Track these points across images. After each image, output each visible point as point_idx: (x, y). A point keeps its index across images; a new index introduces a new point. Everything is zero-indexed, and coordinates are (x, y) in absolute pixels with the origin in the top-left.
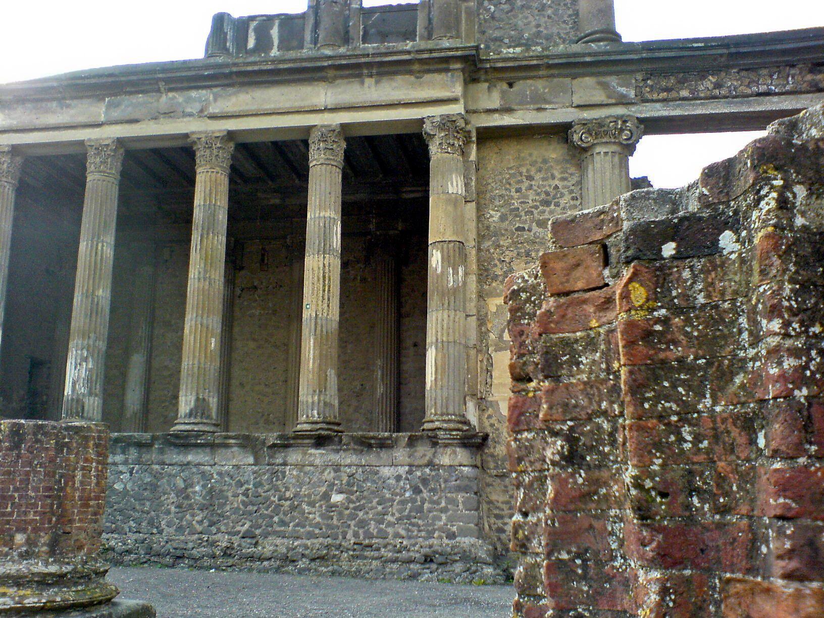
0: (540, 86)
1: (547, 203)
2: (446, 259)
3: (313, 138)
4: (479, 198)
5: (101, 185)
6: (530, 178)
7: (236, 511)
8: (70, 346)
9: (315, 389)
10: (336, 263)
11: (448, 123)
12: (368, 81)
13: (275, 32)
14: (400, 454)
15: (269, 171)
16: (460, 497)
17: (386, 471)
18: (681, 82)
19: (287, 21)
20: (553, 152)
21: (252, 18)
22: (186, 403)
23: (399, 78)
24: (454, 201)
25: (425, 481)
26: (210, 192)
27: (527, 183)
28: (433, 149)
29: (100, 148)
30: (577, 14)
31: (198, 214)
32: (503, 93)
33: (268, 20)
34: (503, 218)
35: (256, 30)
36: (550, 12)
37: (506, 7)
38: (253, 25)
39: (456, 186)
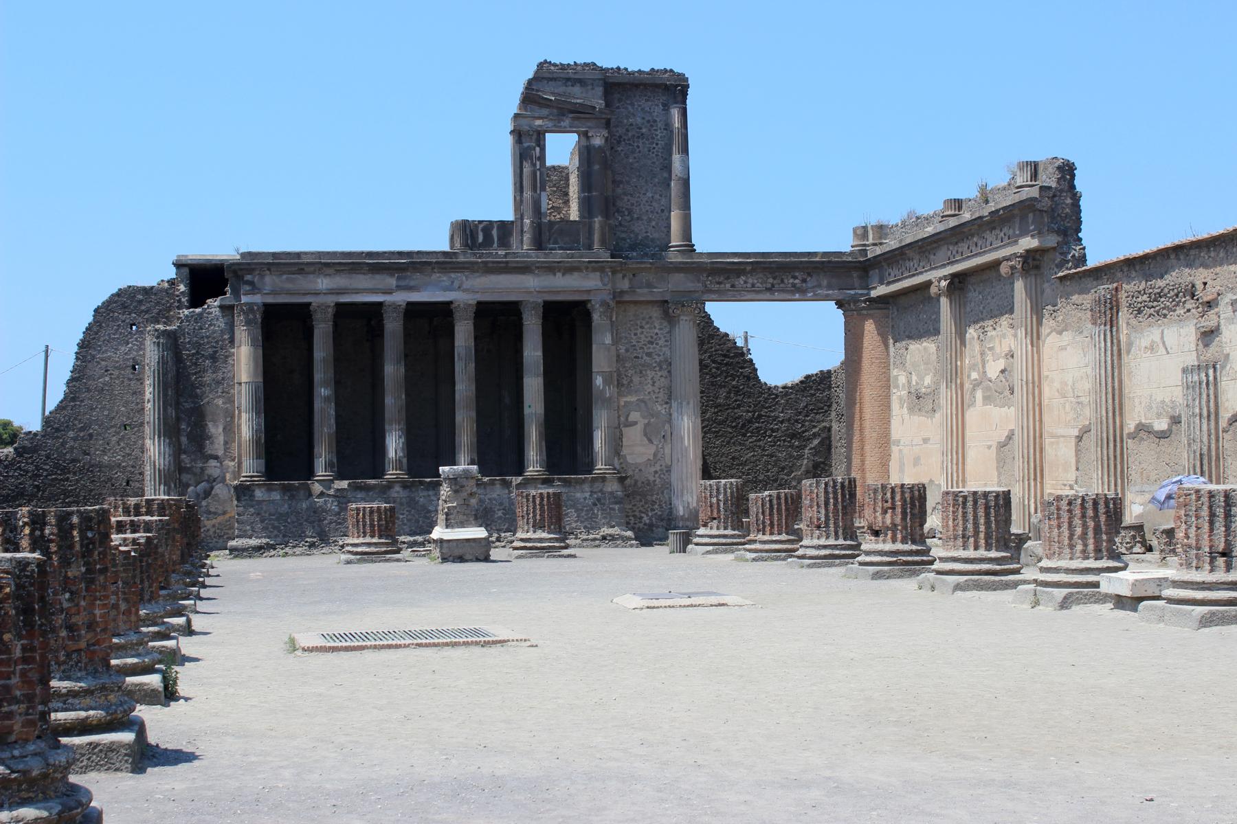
1: (652, 343)
4: (616, 341)
6: (642, 327)
7: (500, 518)
8: (387, 427)
10: (540, 380)
11: (604, 304)
12: (559, 275)
13: (495, 232)
14: (586, 487)
16: (617, 507)
17: (578, 495)
18: (728, 278)
19: (504, 226)
20: (656, 313)
21: (480, 222)
23: (576, 274)
25: (599, 500)
26: (463, 335)
27: (640, 330)
28: (596, 317)
29: (395, 306)
30: (669, 226)
32: (630, 280)
34: (627, 350)
35: (483, 230)
36: (653, 223)
37: (628, 218)
38: (481, 226)
39: (608, 340)
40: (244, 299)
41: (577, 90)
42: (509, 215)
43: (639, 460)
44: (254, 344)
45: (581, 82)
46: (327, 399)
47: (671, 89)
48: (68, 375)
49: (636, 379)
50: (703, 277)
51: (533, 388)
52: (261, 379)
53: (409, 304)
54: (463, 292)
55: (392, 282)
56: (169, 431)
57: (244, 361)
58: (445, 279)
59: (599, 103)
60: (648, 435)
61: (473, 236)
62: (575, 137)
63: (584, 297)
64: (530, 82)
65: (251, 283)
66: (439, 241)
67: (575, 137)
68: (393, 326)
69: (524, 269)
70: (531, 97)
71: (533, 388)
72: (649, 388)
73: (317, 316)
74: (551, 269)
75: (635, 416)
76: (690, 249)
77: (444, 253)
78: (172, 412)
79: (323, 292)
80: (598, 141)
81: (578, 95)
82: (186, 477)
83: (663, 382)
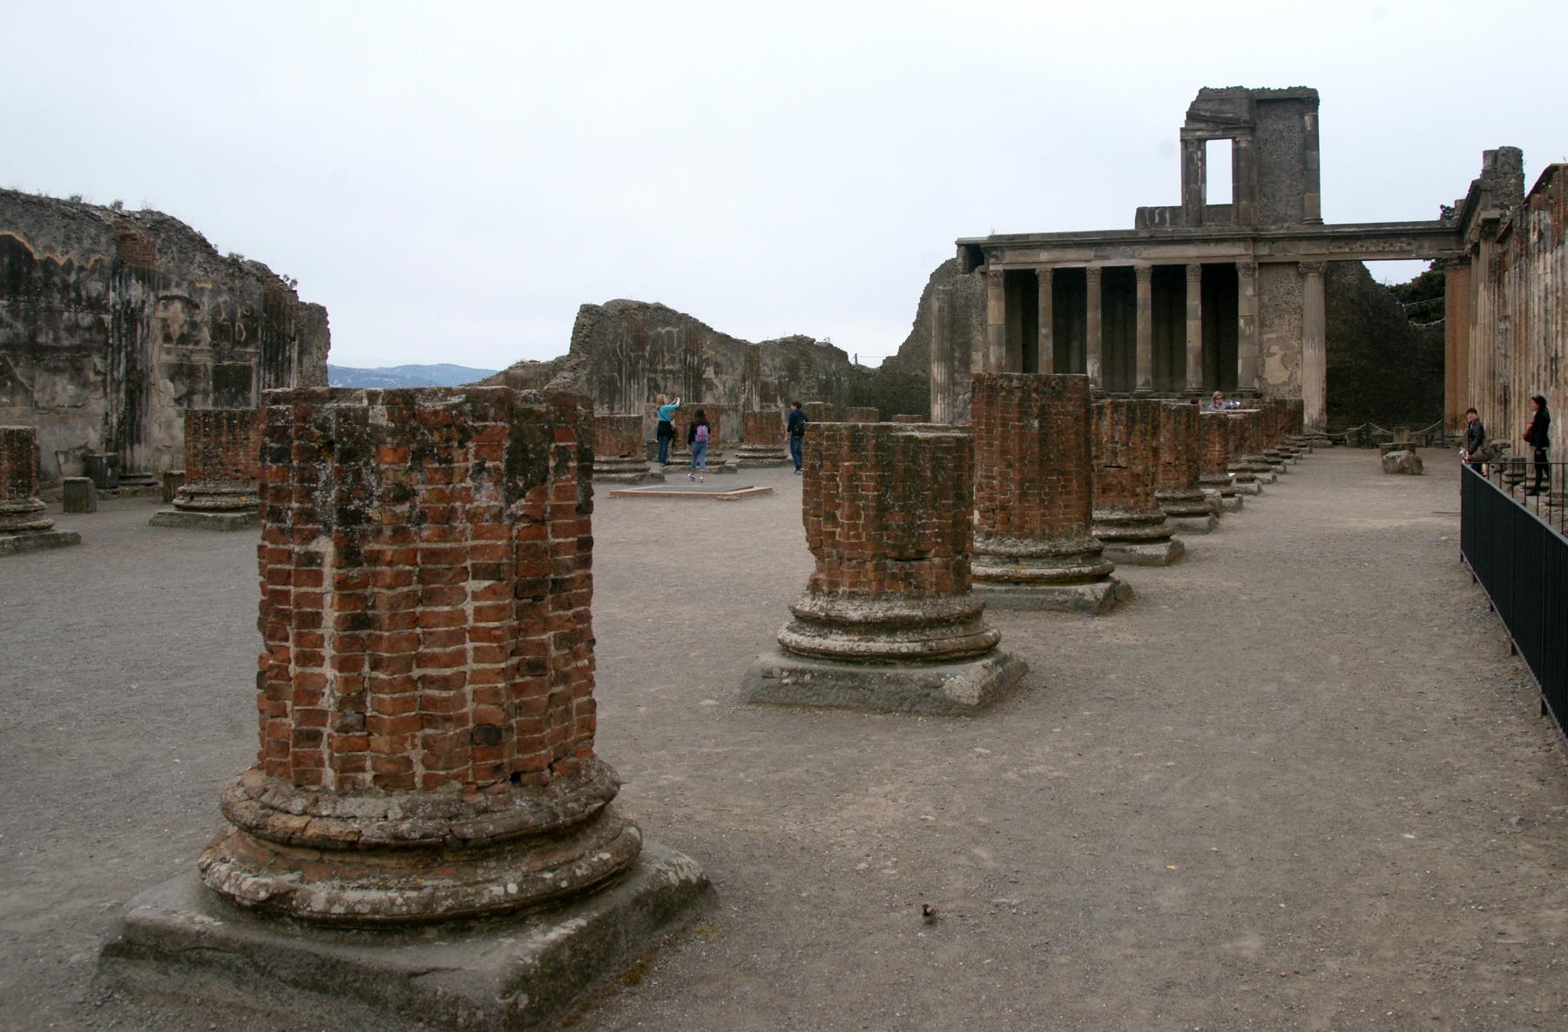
0: (1286, 245)
2: (1246, 323)
3: (1188, 270)
4: (1259, 293)
5: (1094, 287)
9: (1193, 377)
10: (1199, 323)
11: (1247, 267)
15: (1169, 280)
19: (1172, 209)
20: (1292, 271)
22: (1140, 380)
24: (1249, 299)
26: (1143, 290)
31: (1140, 301)
33: (1164, 209)
40: (992, 268)
41: (1227, 107)
42: (1178, 202)
43: (1278, 382)
44: (998, 298)
45: (1230, 101)
46: (1046, 336)
47: (1303, 102)
48: (914, 318)
49: (1277, 321)
50: (1326, 243)
51: (1194, 329)
52: (1002, 322)
53: (1103, 268)
54: (1141, 260)
55: (1090, 254)
56: (947, 358)
57: (996, 311)
58: (1129, 250)
59: (1246, 116)
60: (1284, 362)
61: (1152, 218)
62: (1229, 141)
63: (1231, 260)
64: (1193, 104)
65: (995, 257)
66: (1128, 223)
67: (1229, 141)
68: (1094, 287)
69: (1187, 241)
70: (1192, 115)
71: (1194, 329)
72: (1286, 327)
73: (1041, 279)
74: (1206, 241)
75: (1274, 349)
76: (1319, 221)
77: (1129, 232)
78: (947, 345)
79: (1044, 259)
80: (1243, 145)
81: (1229, 112)
82: (957, 389)
83: (1295, 323)
